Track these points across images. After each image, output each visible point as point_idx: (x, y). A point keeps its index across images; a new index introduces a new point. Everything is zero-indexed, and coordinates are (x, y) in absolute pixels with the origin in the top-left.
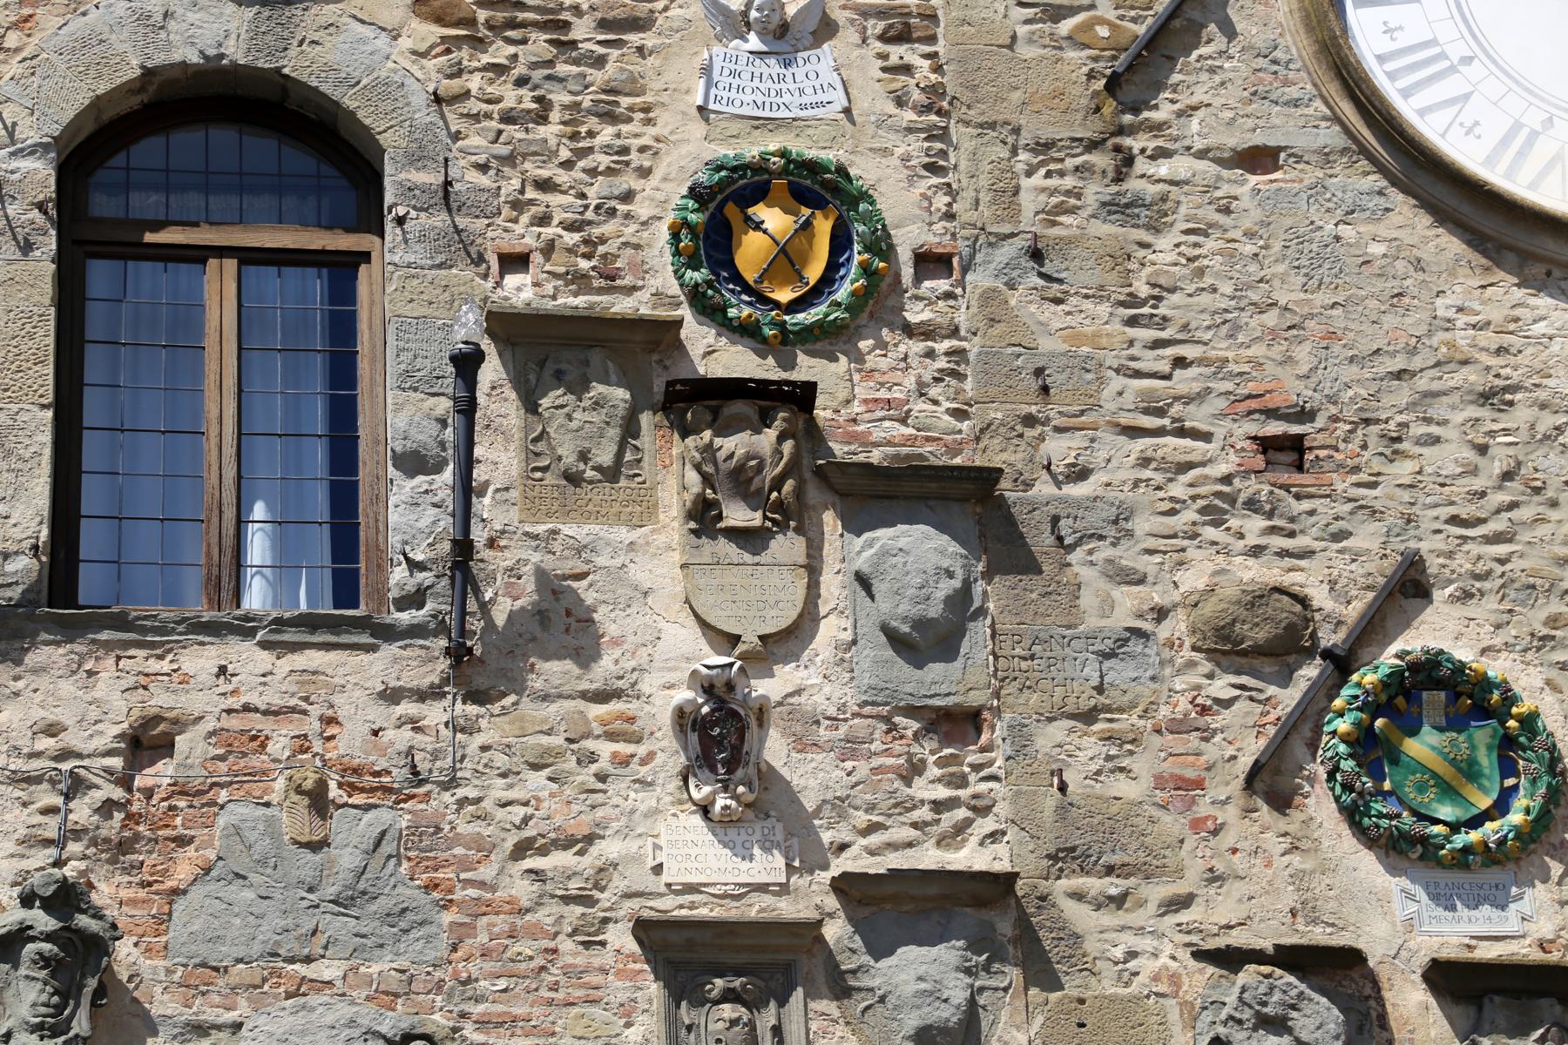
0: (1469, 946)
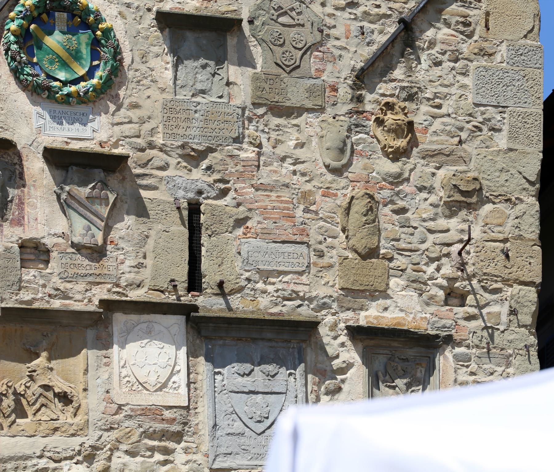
0: (67, 142)
